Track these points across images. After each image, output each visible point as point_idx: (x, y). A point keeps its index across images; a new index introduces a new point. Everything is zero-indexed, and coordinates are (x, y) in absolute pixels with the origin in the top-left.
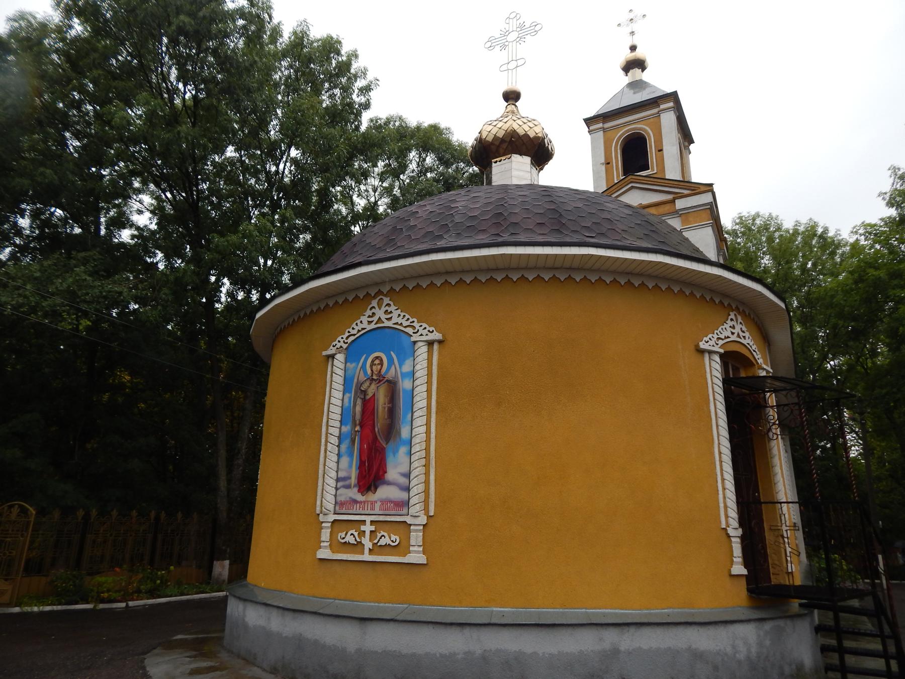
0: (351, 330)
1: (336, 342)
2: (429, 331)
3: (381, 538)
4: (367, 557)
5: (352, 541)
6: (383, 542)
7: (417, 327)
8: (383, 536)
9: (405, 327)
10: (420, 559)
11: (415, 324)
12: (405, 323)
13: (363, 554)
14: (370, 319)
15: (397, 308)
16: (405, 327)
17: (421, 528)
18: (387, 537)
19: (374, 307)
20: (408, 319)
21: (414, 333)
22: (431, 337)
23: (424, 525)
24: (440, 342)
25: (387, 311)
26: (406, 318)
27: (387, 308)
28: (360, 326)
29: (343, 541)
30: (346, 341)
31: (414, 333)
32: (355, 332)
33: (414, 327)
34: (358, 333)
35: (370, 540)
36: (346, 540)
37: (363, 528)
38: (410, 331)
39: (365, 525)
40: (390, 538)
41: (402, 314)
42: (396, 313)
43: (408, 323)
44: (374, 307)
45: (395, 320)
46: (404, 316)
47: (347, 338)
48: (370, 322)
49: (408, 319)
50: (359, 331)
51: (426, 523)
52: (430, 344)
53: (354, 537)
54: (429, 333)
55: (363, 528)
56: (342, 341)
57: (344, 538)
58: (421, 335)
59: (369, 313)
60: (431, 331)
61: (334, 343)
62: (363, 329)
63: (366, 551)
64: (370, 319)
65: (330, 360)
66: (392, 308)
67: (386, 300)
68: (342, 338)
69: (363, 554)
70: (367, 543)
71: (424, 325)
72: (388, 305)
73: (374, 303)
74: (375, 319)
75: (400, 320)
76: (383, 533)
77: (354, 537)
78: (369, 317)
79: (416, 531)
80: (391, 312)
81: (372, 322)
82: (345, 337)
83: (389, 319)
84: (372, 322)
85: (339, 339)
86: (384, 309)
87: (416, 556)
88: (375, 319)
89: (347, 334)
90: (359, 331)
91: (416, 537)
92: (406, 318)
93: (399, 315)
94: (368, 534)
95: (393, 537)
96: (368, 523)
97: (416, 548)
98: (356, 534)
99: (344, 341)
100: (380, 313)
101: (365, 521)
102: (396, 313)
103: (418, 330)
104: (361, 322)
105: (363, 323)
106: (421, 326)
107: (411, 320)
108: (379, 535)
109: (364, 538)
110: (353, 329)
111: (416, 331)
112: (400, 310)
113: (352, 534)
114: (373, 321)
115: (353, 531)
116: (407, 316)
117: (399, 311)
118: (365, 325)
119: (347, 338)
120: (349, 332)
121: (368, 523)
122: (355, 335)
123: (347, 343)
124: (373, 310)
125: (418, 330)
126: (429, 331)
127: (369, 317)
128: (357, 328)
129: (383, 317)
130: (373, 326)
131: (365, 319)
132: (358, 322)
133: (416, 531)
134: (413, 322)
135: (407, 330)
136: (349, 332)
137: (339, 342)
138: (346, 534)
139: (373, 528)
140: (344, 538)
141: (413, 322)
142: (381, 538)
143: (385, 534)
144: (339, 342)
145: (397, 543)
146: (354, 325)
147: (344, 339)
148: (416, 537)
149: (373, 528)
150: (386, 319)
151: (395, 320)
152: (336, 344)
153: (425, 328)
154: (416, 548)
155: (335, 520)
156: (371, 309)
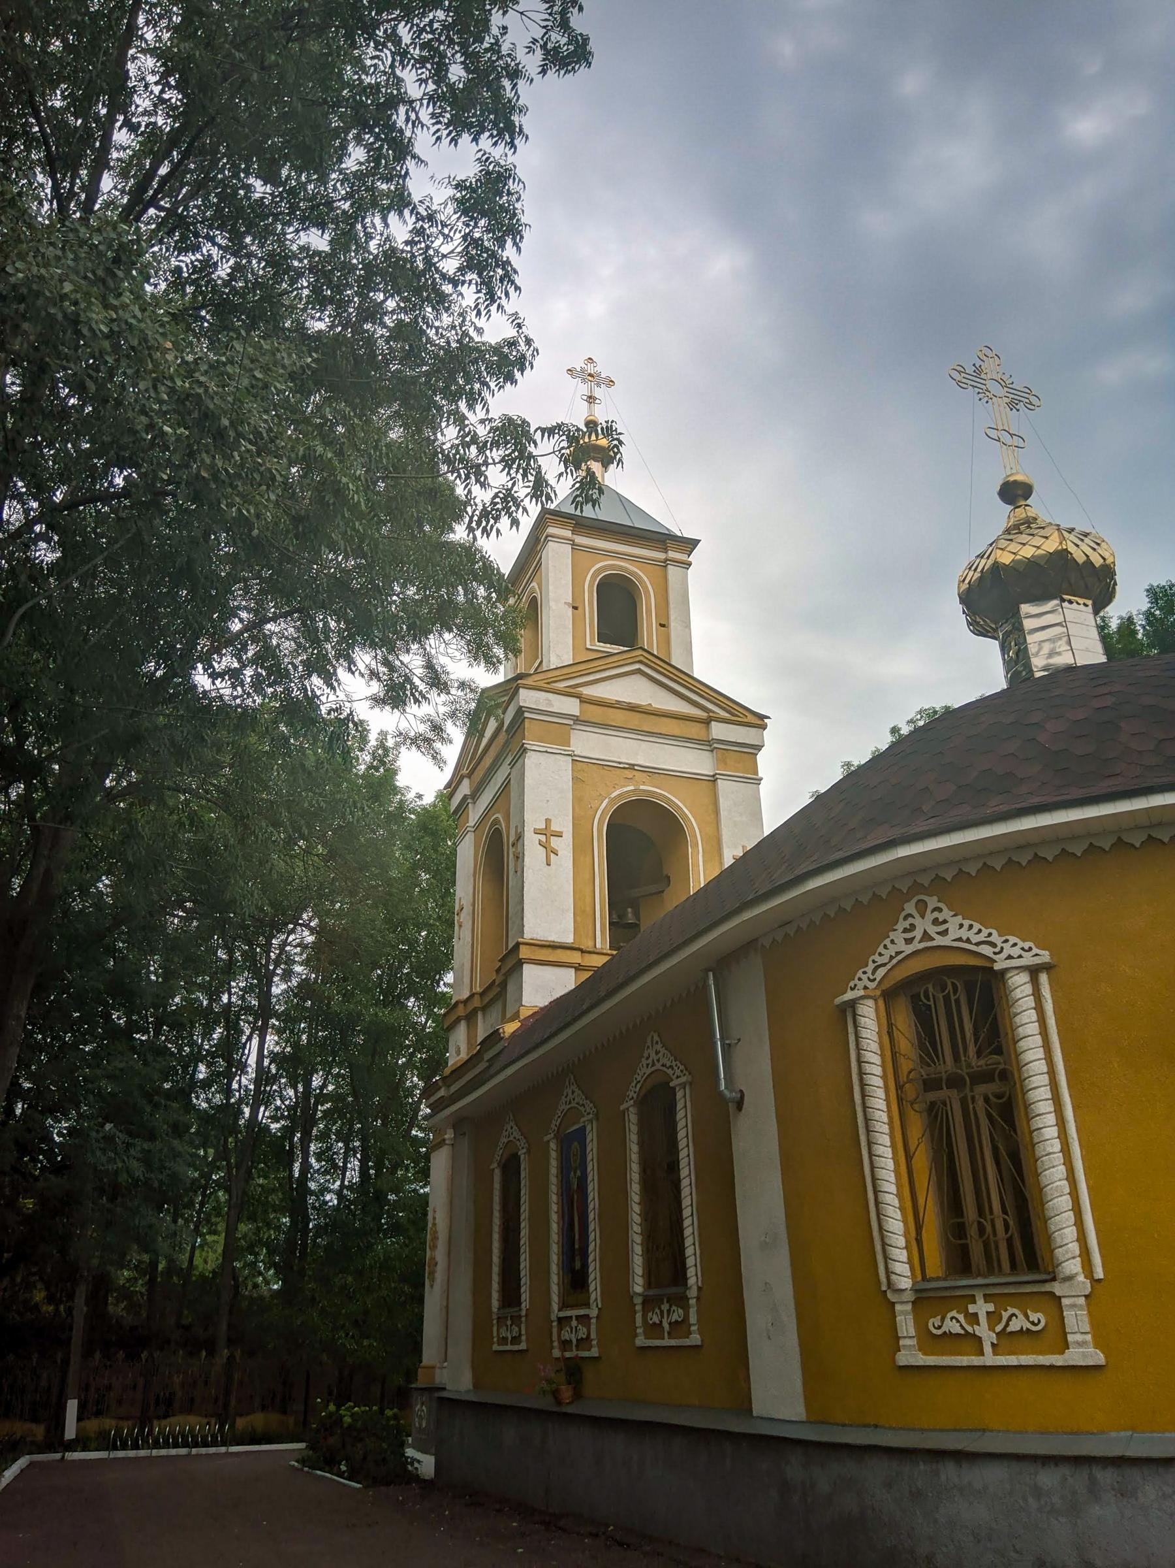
0: (876, 957)
2: (1023, 949)
3: (1010, 1319)
4: (989, 1359)
5: (957, 1329)
6: (1015, 1326)
7: (1000, 945)
8: (1013, 1315)
9: (978, 944)
11: (995, 938)
12: (975, 939)
14: (908, 935)
15: (953, 913)
16: (978, 944)
17: (1082, 1301)
18: (1021, 1316)
19: (910, 915)
20: (980, 931)
21: (995, 953)
22: (1028, 960)
23: (1086, 1297)
26: (975, 930)
27: (936, 914)
28: (892, 950)
29: (939, 1332)
30: (872, 977)
31: (995, 953)
32: (885, 959)
33: (994, 945)
34: (890, 962)
35: (992, 1329)
36: (944, 1329)
37: (972, 1309)
38: (986, 950)
39: (975, 1302)
41: (966, 923)
42: (953, 923)
43: (981, 937)
44: (910, 915)
45: (954, 933)
46: (971, 927)
47: (874, 972)
48: (909, 941)
49: (980, 931)
50: (892, 958)
51: (1091, 1292)
52: (1034, 972)
53: (958, 1321)
54: (1023, 953)
55: (972, 1309)
56: (864, 977)
57: (939, 1327)
58: (1010, 957)
59: (902, 925)
60: (1026, 948)
61: (852, 984)
62: (898, 953)
63: (988, 1349)
64: (908, 935)
66: (946, 913)
67: (932, 902)
68: (865, 973)
70: (983, 1330)
72: (940, 910)
73: (910, 908)
74: (918, 934)
75: (964, 934)
76: (1011, 1311)
77: (958, 1321)
78: (905, 931)
79: (1073, 1306)
80: (945, 922)
82: (869, 969)
83: (944, 933)
84: (914, 938)
85: (860, 974)
86: (930, 916)
88: (918, 934)
89: (871, 966)
90: (892, 958)
91: (1077, 1320)
92: (975, 930)
93: (961, 926)
94: (983, 1319)
99: (869, 978)
100: (923, 925)
102: (953, 923)
103: (1002, 948)
104: (892, 942)
105: (897, 944)
106: (1006, 941)
108: (1005, 1315)
109: (979, 1325)
110: (880, 955)
111: (997, 950)
112: (960, 917)
113: (952, 1318)
114: (914, 938)
115: (954, 1313)
116: (977, 926)
117: (959, 919)
118: (901, 945)
119: (874, 972)
120: (874, 962)
122: (884, 965)
123: (875, 979)
124: (910, 920)
125: (1002, 948)
126: (1023, 949)
127: (905, 931)
128: (887, 954)
129: (932, 930)
130: (917, 946)
131: (898, 936)
132: (887, 942)
133: (1073, 1306)
134: (990, 935)
136: (874, 962)
137: (860, 979)
138: (943, 1320)
139: (991, 1307)
140: (939, 1327)
141: (990, 935)
142: (1010, 1319)
145: (1039, 1327)
146: (881, 949)
149: (991, 1307)
150: (938, 933)
151: (954, 933)
152: (855, 985)
153: (1015, 945)
156: (905, 918)
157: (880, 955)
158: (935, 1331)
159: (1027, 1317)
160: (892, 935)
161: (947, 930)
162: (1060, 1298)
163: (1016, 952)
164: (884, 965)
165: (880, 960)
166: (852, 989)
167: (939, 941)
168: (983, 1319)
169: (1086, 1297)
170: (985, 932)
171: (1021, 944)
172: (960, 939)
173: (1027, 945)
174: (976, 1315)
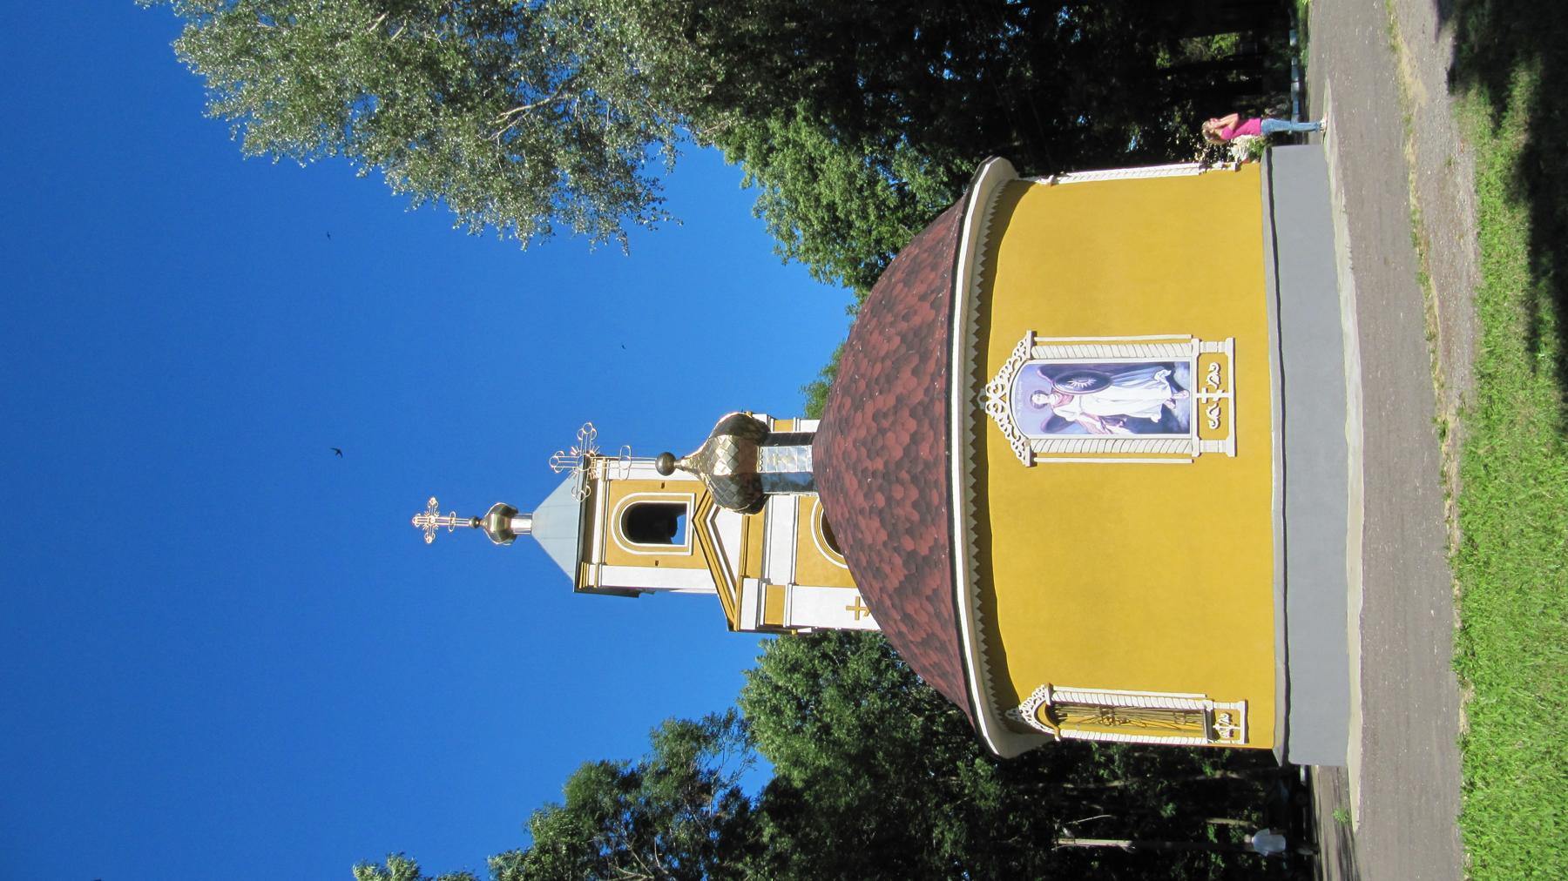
1: (1017, 451)
4: (1230, 395)
5: (1216, 412)
6: (1216, 379)
7: (1016, 357)
10: (1230, 340)
12: (1010, 369)
13: (1227, 398)
14: (1000, 409)
22: (1028, 344)
24: (1034, 334)
25: (994, 391)
27: (991, 391)
28: (1005, 421)
29: (1217, 423)
33: (1016, 360)
35: (1215, 392)
36: (1215, 419)
38: (1017, 366)
40: (1211, 372)
41: (1000, 373)
45: (1004, 381)
50: (1009, 422)
52: (1034, 344)
53: (1212, 410)
55: (1204, 401)
58: (1024, 353)
63: (1224, 395)
65: (1035, 459)
69: (1227, 398)
70: (1216, 395)
71: (1015, 351)
75: (1006, 376)
77: (1212, 410)
78: (996, 411)
81: (1003, 407)
84: (1003, 407)
87: (1227, 347)
88: (1000, 403)
91: (1210, 347)
92: (1005, 370)
94: (1209, 395)
95: (1212, 368)
96: (1199, 395)
97: (1220, 347)
98: (1210, 408)
101: (1198, 399)
102: (999, 381)
104: (1000, 420)
107: (1007, 364)
110: (1006, 430)
116: (1004, 368)
117: (997, 377)
118: (1004, 415)
120: (1009, 436)
121: (1199, 395)
122: (1013, 428)
123: (1020, 437)
127: (996, 411)
128: (1007, 425)
129: (1000, 393)
130: (1007, 406)
132: (999, 424)
133: (1205, 346)
135: (1017, 367)
136: (1009, 436)
137: (1017, 448)
139: (1204, 390)
141: (1010, 362)
143: (1209, 376)
144: (1017, 448)
146: (1002, 429)
147: (1015, 440)
148: (1210, 347)
150: (1003, 389)
154: (1220, 347)
155: (1198, 435)
157: (1006, 430)
158: (1216, 426)
159: (1211, 372)
160: (997, 420)
161: (1002, 386)
162: (1200, 354)
163: (1022, 350)
164: (1013, 428)
165: (1009, 431)
166: (1020, 456)
167: (1007, 390)
168: (1209, 395)
169: (1200, 341)
170: (1007, 364)
171: (1018, 347)
172: (1009, 379)
173: (1019, 344)
174: (1207, 399)
